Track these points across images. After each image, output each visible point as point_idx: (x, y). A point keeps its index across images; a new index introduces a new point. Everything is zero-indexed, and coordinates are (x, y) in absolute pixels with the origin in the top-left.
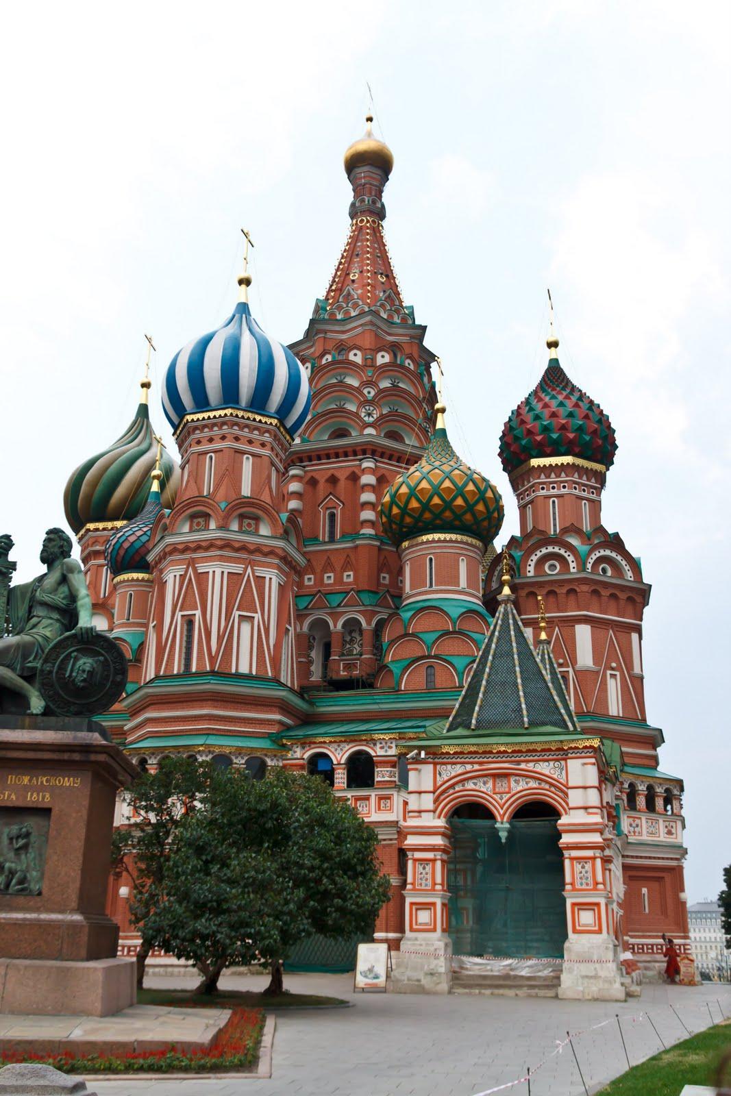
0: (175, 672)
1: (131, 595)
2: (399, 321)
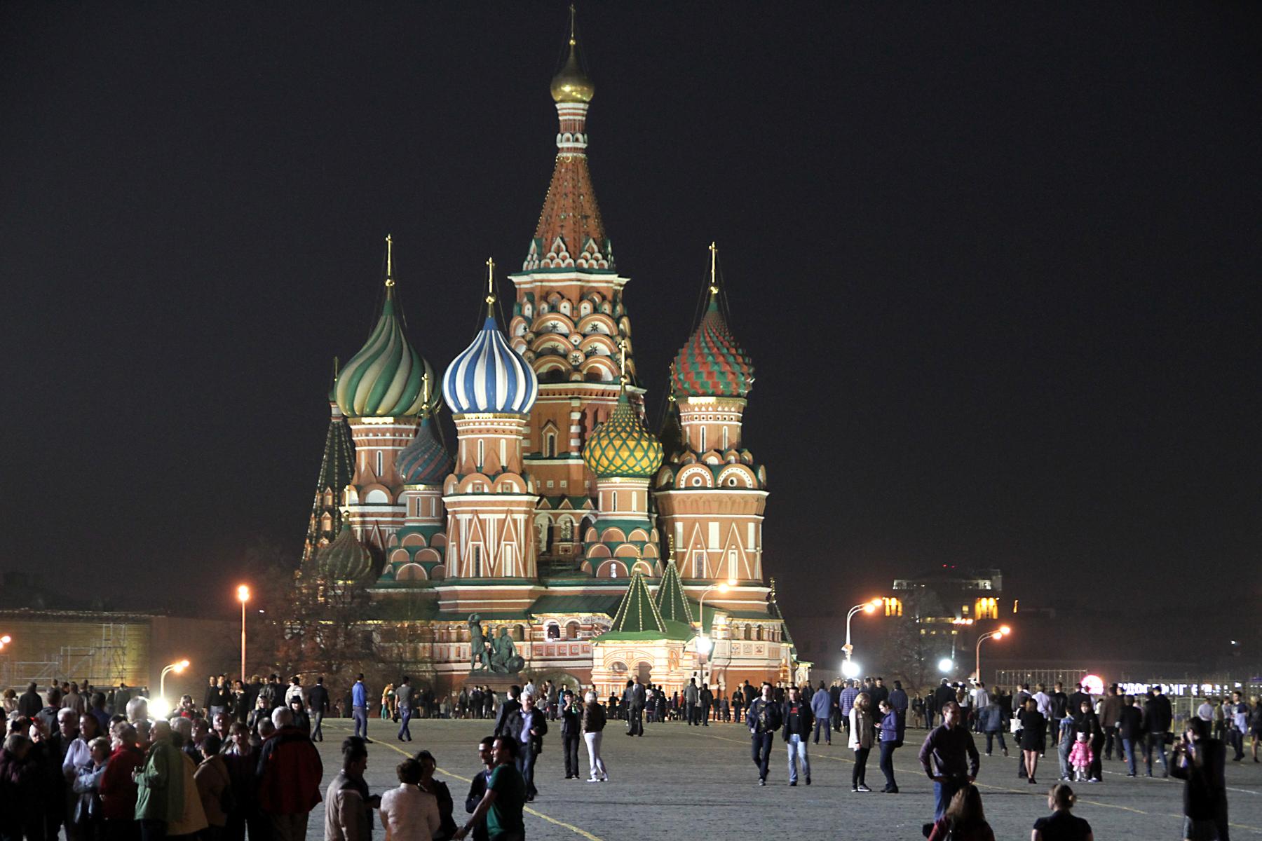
0: (471, 576)
1: (418, 499)
2: (597, 268)
